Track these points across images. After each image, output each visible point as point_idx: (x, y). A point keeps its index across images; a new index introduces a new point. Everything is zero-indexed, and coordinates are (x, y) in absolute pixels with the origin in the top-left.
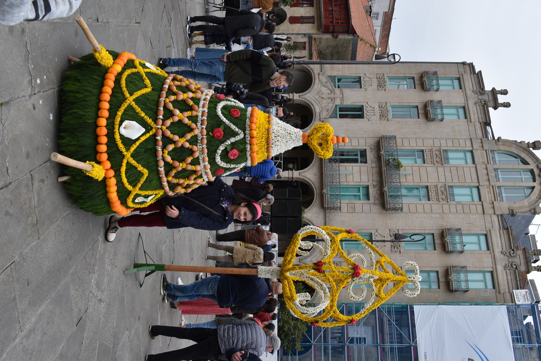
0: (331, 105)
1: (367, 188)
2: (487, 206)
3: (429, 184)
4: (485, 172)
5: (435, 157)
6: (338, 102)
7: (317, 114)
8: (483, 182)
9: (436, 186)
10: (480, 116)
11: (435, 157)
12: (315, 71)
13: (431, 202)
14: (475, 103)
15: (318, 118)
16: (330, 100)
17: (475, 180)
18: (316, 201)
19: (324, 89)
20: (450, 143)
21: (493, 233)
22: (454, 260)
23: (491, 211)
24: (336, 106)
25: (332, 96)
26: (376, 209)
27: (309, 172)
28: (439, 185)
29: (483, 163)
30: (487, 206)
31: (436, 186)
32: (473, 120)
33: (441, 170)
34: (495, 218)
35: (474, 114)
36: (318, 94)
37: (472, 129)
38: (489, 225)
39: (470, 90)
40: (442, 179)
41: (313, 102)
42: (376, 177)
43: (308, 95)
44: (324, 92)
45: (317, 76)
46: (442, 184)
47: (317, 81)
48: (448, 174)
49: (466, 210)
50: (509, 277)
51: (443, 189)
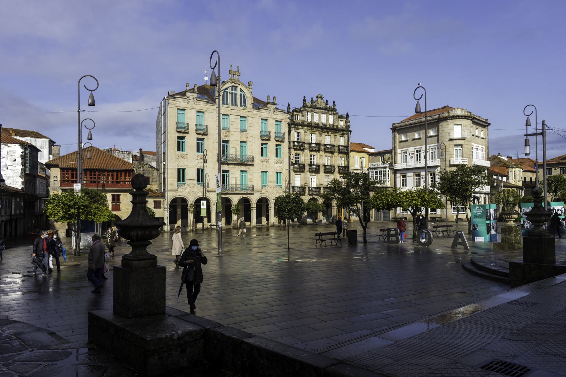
1: (242, 171)
3: (240, 141)
4: (233, 111)
5: (227, 135)
6: (195, 182)
10: (203, 104)
11: (227, 135)
12: (174, 195)
13: (248, 141)
16: (194, 187)
18: (248, 196)
19: (187, 190)
21: (261, 115)
22: (273, 136)
25: (192, 186)
27: (234, 199)
31: (241, 137)
33: (232, 133)
34: (254, 112)
36: (190, 194)
37: (210, 111)
39: (186, 105)
40: (238, 133)
41: (195, 197)
42: (237, 167)
43: (191, 200)
45: (178, 194)
47: (181, 194)
48: (234, 130)
49: (251, 125)
50: (278, 114)
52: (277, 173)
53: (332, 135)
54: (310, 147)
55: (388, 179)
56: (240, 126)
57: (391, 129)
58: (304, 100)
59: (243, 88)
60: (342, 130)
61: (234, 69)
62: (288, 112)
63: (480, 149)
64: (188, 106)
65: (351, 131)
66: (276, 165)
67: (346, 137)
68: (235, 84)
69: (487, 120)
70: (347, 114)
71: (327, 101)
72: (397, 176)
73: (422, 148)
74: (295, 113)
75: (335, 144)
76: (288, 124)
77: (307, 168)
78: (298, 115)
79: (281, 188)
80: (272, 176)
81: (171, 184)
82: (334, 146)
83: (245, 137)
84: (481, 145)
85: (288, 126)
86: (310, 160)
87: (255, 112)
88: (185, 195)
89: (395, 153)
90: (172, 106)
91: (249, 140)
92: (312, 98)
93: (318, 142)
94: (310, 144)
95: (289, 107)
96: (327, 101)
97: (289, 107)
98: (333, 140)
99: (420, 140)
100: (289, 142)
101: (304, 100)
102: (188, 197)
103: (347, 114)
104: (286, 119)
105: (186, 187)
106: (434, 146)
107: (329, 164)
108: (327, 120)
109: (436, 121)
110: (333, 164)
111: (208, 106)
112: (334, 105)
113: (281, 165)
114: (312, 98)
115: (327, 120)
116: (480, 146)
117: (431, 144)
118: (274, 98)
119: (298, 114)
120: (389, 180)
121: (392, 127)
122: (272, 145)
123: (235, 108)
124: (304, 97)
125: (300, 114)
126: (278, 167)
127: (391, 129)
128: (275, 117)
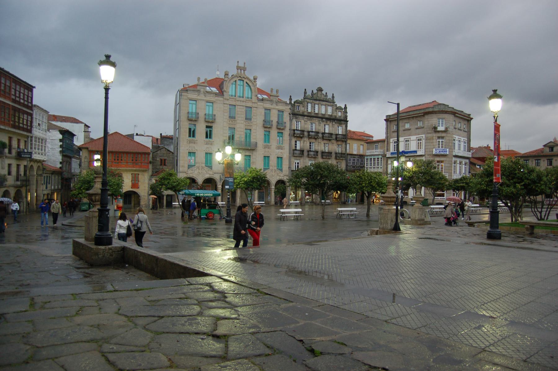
0: (205, 169)
2: (254, 105)
6: (204, 165)
7: (210, 176)
8: (244, 104)
9: (246, 125)
14: (205, 96)
15: (212, 176)
17: (243, 107)
19: (196, 172)
20: (226, 114)
23: (256, 104)
24: (205, 166)
25: (200, 168)
26: (254, 153)
28: (245, 123)
29: (235, 101)
30: (254, 105)
31: (246, 125)
32: (214, 100)
33: (238, 121)
35: (211, 98)
38: (261, 107)
39: (197, 97)
41: (204, 178)
44: (197, 171)
46: (245, 122)
47: (191, 175)
48: (240, 119)
51: (247, 123)
52: (278, 157)
53: (331, 124)
54: (309, 135)
55: (381, 165)
56: (245, 115)
57: (385, 120)
58: (305, 93)
59: (248, 82)
60: (341, 120)
61: (241, 64)
62: (291, 103)
63: (462, 141)
64: (199, 98)
65: (348, 121)
66: (277, 151)
67: (344, 126)
68: (241, 78)
69: (470, 115)
70: (346, 105)
71: (326, 93)
72: (389, 163)
73: (410, 138)
74: (296, 104)
75: (333, 133)
76: (290, 114)
77: (306, 153)
78: (299, 106)
79: (282, 171)
80: (273, 161)
81: (183, 166)
82: (331, 134)
83: (249, 126)
84: (463, 137)
85: (289, 115)
86: (309, 147)
87: (259, 103)
88: (194, 176)
89: (388, 144)
90: (185, 97)
91: (253, 128)
92: (312, 91)
93: (317, 131)
94: (309, 132)
95: (291, 99)
96: (326, 93)
97: (291, 99)
98: (331, 128)
99: (409, 131)
100: (290, 130)
101: (305, 93)
102: (197, 177)
103: (346, 105)
104: (287, 110)
105: (196, 168)
106: (420, 137)
107: (327, 151)
108: (326, 111)
109: (422, 114)
110: (330, 150)
111: (217, 98)
112: (333, 97)
113: (281, 151)
114: (312, 91)
115: (326, 111)
116: (462, 139)
117: (418, 135)
118: (277, 91)
119: (298, 105)
120: (382, 166)
121: (385, 118)
122: (274, 132)
123: (242, 99)
124: (305, 90)
125: (301, 105)
126: (278, 152)
127: (385, 120)
128: (277, 107)
